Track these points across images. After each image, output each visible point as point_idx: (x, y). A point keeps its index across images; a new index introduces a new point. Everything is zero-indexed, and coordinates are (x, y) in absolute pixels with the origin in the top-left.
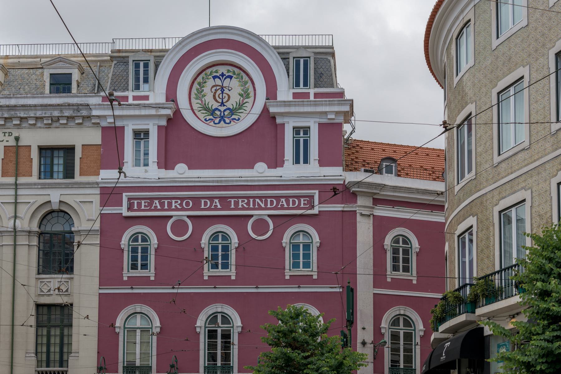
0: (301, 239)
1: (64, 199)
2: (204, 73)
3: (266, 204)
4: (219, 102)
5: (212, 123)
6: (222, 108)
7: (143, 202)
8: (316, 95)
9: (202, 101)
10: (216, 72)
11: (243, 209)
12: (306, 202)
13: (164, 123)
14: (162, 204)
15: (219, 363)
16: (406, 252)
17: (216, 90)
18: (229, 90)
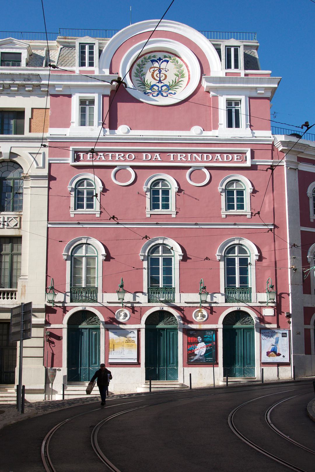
0: (234, 187)
1: (14, 151)
2: (143, 57)
5: (151, 96)
6: (160, 85)
8: (246, 75)
9: (141, 79)
10: (154, 57)
11: (181, 161)
17: (154, 71)
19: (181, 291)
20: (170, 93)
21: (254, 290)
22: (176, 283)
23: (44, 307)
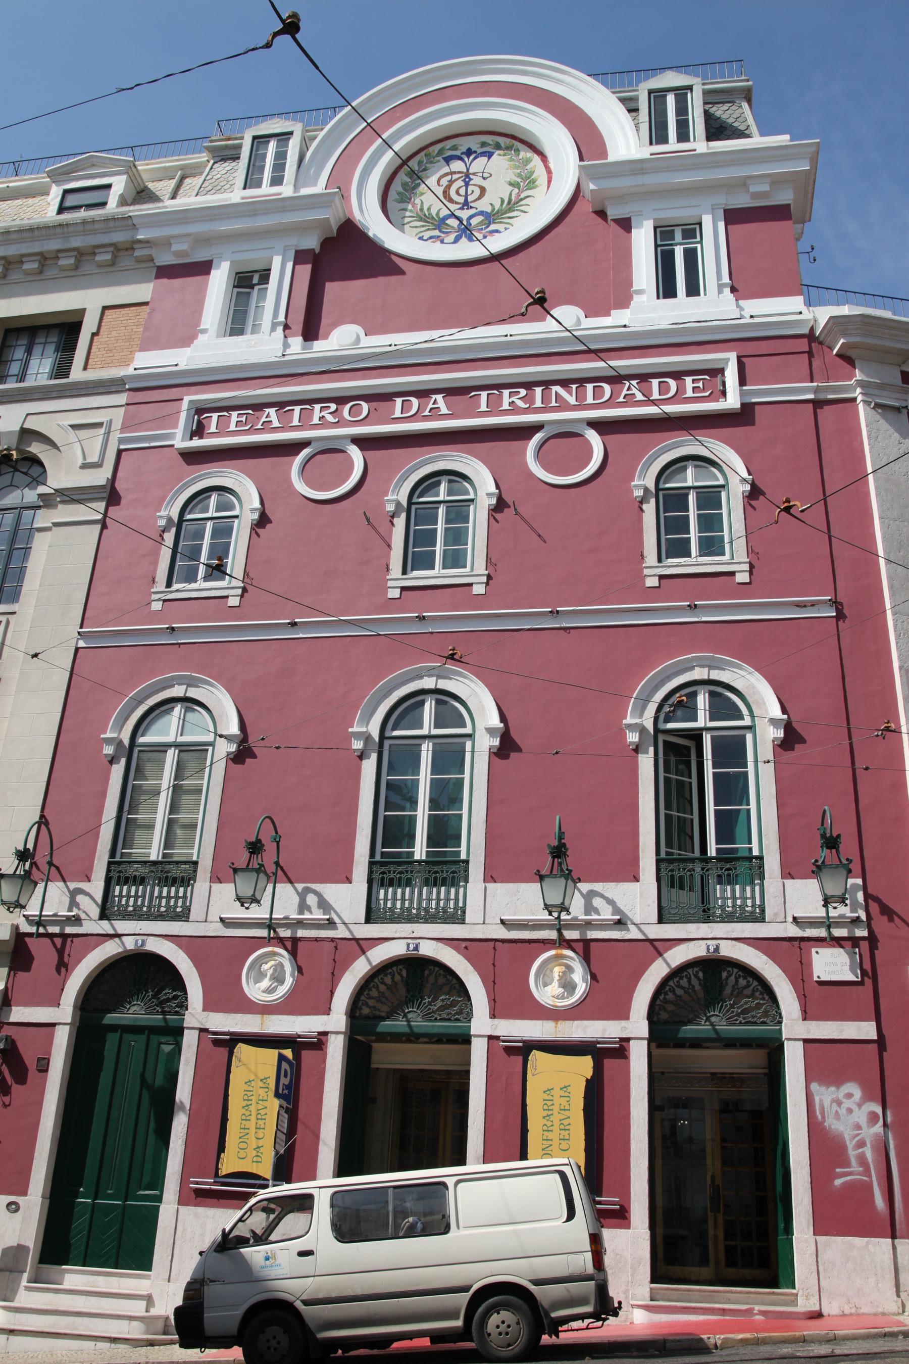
0: (690, 477)
1: (30, 424)
2: (423, 154)
3: (581, 396)
4: (457, 203)
6: (464, 214)
10: (454, 148)
12: (700, 384)
13: (312, 242)
14: (285, 417)
15: (420, 850)
17: (451, 182)
18: (484, 179)
19: (490, 877)
21: (772, 864)
22: (473, 844)
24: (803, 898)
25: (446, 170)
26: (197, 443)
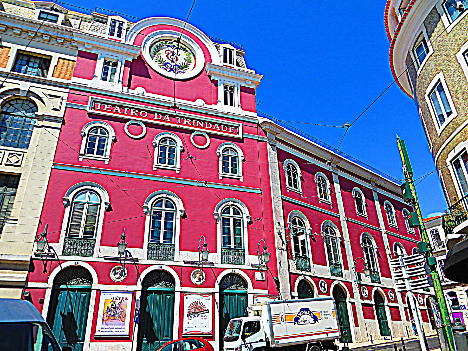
0: (230, 153)
1: (32, 89)
3: (204, 125)
6: (173, 64)
7: (106, 106)
9: (158, 56)
11: (187, 125)
13: (131, 60)
16: (294, 176)
17: (169, 53)
20: (180, 72)
23: (29, 259)
24: (254, 260)
25: (167, 49)
26: (93, 111)
